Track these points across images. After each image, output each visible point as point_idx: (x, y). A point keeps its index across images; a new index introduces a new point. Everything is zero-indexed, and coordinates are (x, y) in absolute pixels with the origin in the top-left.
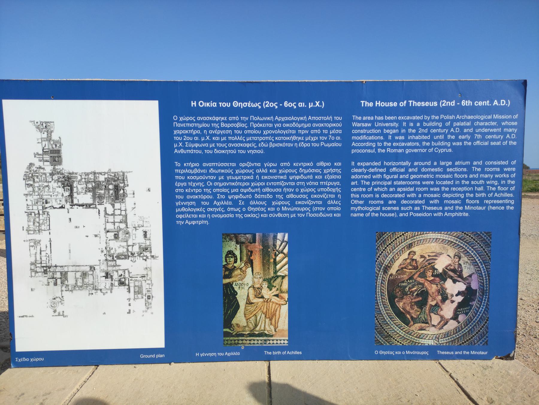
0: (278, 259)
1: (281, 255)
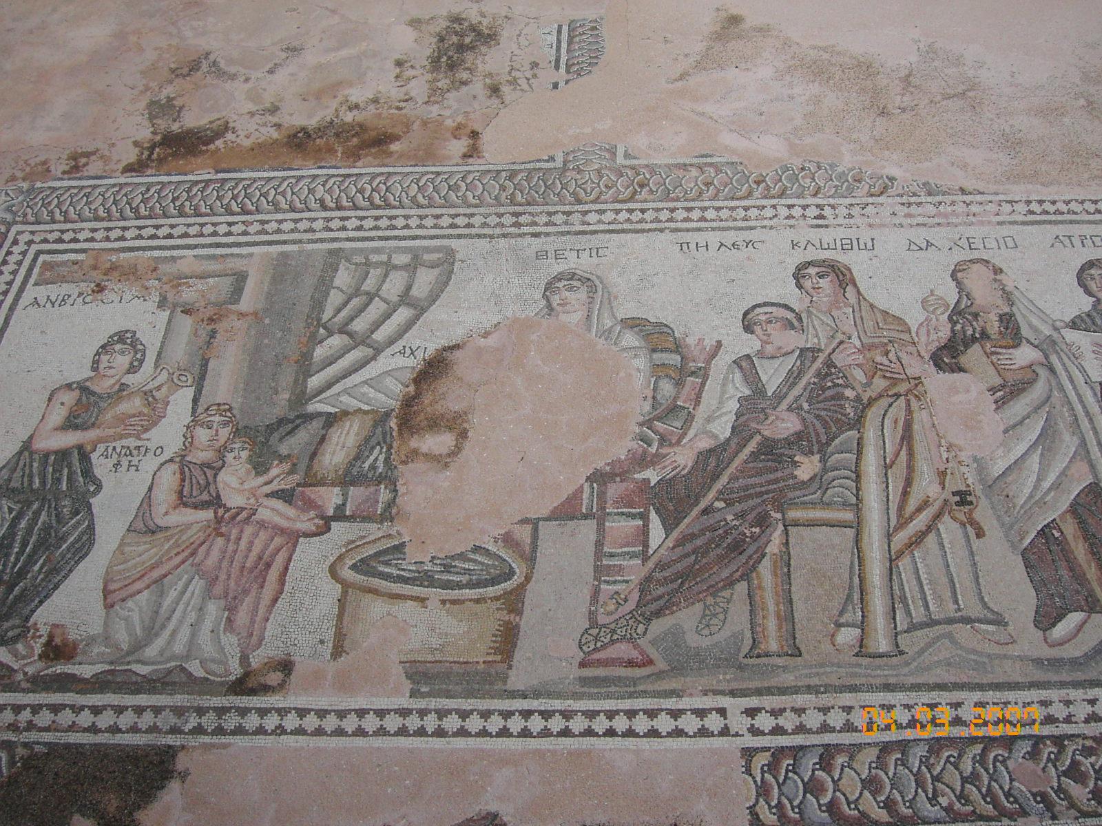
0: (319, 353)
1: (336, 341)
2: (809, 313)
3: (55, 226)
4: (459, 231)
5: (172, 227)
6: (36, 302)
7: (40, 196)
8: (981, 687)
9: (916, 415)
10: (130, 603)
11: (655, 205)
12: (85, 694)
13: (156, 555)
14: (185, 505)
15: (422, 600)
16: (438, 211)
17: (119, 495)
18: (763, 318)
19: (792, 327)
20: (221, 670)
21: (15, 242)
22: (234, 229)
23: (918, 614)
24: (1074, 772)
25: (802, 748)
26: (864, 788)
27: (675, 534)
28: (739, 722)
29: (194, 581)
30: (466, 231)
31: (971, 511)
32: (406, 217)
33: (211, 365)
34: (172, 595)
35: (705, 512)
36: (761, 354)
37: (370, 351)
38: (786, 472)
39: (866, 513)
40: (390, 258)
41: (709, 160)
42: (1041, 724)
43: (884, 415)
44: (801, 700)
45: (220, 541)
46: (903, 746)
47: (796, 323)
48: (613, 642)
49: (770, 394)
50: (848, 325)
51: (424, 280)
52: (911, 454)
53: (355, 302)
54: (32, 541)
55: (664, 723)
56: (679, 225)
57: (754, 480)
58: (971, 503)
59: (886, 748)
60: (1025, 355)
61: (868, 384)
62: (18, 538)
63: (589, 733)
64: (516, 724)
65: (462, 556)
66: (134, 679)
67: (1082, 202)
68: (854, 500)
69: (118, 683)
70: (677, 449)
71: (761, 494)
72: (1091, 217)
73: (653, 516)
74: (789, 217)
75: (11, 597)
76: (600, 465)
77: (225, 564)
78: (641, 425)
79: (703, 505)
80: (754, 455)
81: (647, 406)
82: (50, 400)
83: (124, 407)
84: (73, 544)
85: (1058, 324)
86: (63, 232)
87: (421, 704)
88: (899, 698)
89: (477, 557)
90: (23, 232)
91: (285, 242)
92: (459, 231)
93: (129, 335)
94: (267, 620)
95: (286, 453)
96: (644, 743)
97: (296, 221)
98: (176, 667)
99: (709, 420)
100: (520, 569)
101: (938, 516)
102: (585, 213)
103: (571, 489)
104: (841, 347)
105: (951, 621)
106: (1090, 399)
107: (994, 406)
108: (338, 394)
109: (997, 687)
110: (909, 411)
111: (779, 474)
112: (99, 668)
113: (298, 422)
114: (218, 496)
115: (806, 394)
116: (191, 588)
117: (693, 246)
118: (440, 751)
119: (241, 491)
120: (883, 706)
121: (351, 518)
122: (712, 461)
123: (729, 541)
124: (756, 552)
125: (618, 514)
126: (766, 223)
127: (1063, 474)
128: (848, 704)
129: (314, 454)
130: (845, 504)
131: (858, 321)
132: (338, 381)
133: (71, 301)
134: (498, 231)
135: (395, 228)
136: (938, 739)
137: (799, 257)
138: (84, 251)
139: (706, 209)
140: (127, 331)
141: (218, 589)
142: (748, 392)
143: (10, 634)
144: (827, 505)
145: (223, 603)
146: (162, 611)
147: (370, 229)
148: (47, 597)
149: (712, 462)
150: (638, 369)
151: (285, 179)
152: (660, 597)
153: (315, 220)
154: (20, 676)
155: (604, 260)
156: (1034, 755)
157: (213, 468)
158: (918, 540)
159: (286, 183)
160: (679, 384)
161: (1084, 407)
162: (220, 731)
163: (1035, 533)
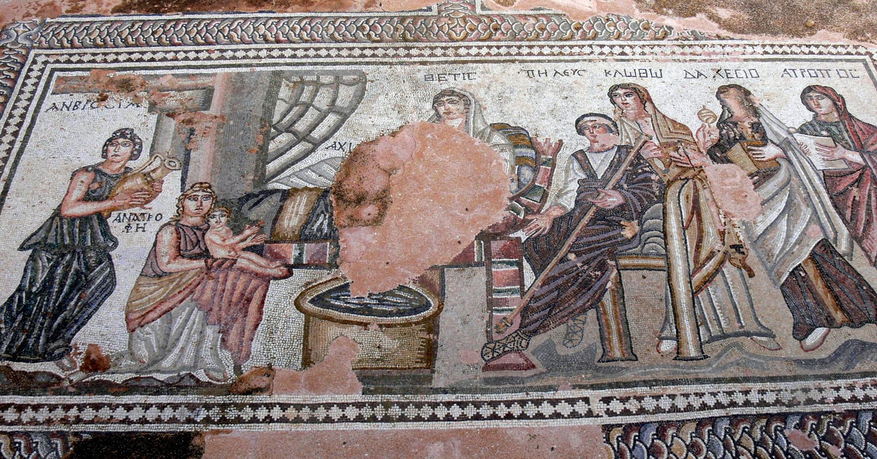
0: (272, 146)
1: (284, 138)
2: (622, 122)
3: (64, 51)
4: (367, 60)
5: (154, 53)
6: (54, 106)
7: (51, 29)
8: (762, 380)
9: (701, 193)
10: (147, 329)
11: (506, 43)
12: (118, 395)
13: (164, 293)
14: (183, 257)
15: (365, 325)
16: (351, 45)
17: (132, 248)
18: (590, 124)
19: (612, 131)
20: (221, 377)
21: (34, 62)
22: (201, 55)
23: (715, 331)
24: (829, 437)
25: (643, 424)
26: (688, 451)
27: (542, 276)
28: (598, 407)
29: (194, 312)
30: (373, 60)
31: (744, 259)
32: (328, 49)
33: (192, 154)
34: (179, 321)
35: (562, 260)
36: (590, 149)
37: (310, 146)
38: (615, 233)
39: (673, 261)
40: (318, 78)
41: (541, 12)
42: (805, 404)
43: (679, 193)
44: (640, 390)
45: (211, 283)
46: (713, 421)
47: (613, 129)
48: (505, 352)
49: (599, 178)
50: (649, 130)
51: (345, 94)
52: (700, 220)
53: (296, 109)
54: (69, 282)
55: (547, 409)
56: (525, 58)
57: (594, 238)
58: (743, 253)
59: (701, 423)
60: (770, 151)
61: (667, 171)
62: (57, 281)
63: (494, 417)
64: (441, 412)
65: (391, 293)
66: (155, 384)
67: (800, 46)
68: (664, 252)
69: (143, 387)
70: (538, 216)
71: (599, 248)
72: (807, 57)
73: (525, 263)
74: (601, 54)
75: (56, 324)
76: (485, 228)
77: (216, 299)
78: (511, 199)
79: (560, 254)
80: (593, 221)
81: (514, 186)
82: (72, 179)
83: (128, 185)
84: (99, 285)
85: (791, 130)
86: (71, 55)
87: (372, 399)
88: (707, 388)
89: (402, 294)
90: (40, 55)
91: (240, 66)
92: (367, 60)
93: (127, 132)
94: (252, 340)
95: (255, 219)
96: (534, 423)
97: (246, 50)
98: (187, 374)
99: (558, 196)
100: (434, 303)
101: (722, 263)
102: (457, 48)
103: (464, 245)
104: (646, 145)
105: (737, 335)
106: (817, 182)
107: (753, 187)
108: (289, 176)
109: (772, 379)
110: (696, 190)
111: (611, 234)
112: (129, 376)
113: (261, 196)
114: (207, 250)
115: (625, 177)
116: (192, 317)
117: (536, 73)
118: (389, 432)
119: (224, 247)
120: (696, 394)
121: (308, 266)
122: (563, 224)
123: (580, 281)
124: (599, 288)
125: (500, 262)
126: (585, 57)
127: (804, 233)
128: (672, 393)
129: (276, 220)
130: (658, 255)
131: (656, 127)
132: (288, 167)
133: (82, 106)
134: (395, 60)
135: (320, 56)
136: (736, 416)
137: (610, 82)
138: (88, 69)
139: (543, 47)
140: (126, 129)
141: (213, 318)
142: (584, 177)
143: (57, 352)
144: (646, 256)
145: (217, 328)
146: (173, 333)
147: (302, 57)
148: (83, 324)
149: (564, 225)
150: (506, 160)
151: (235, 19)
152: (537, 320)
153: (261, 49)
154: (67, 383)
155: (473, 82)
156: (801, 426)
157: (200, 230)
158: (708, 280)
159: (236, 23)
160: (536, 170)
161: (813, 187)
162: (224, 421)
163: (788, 274)
